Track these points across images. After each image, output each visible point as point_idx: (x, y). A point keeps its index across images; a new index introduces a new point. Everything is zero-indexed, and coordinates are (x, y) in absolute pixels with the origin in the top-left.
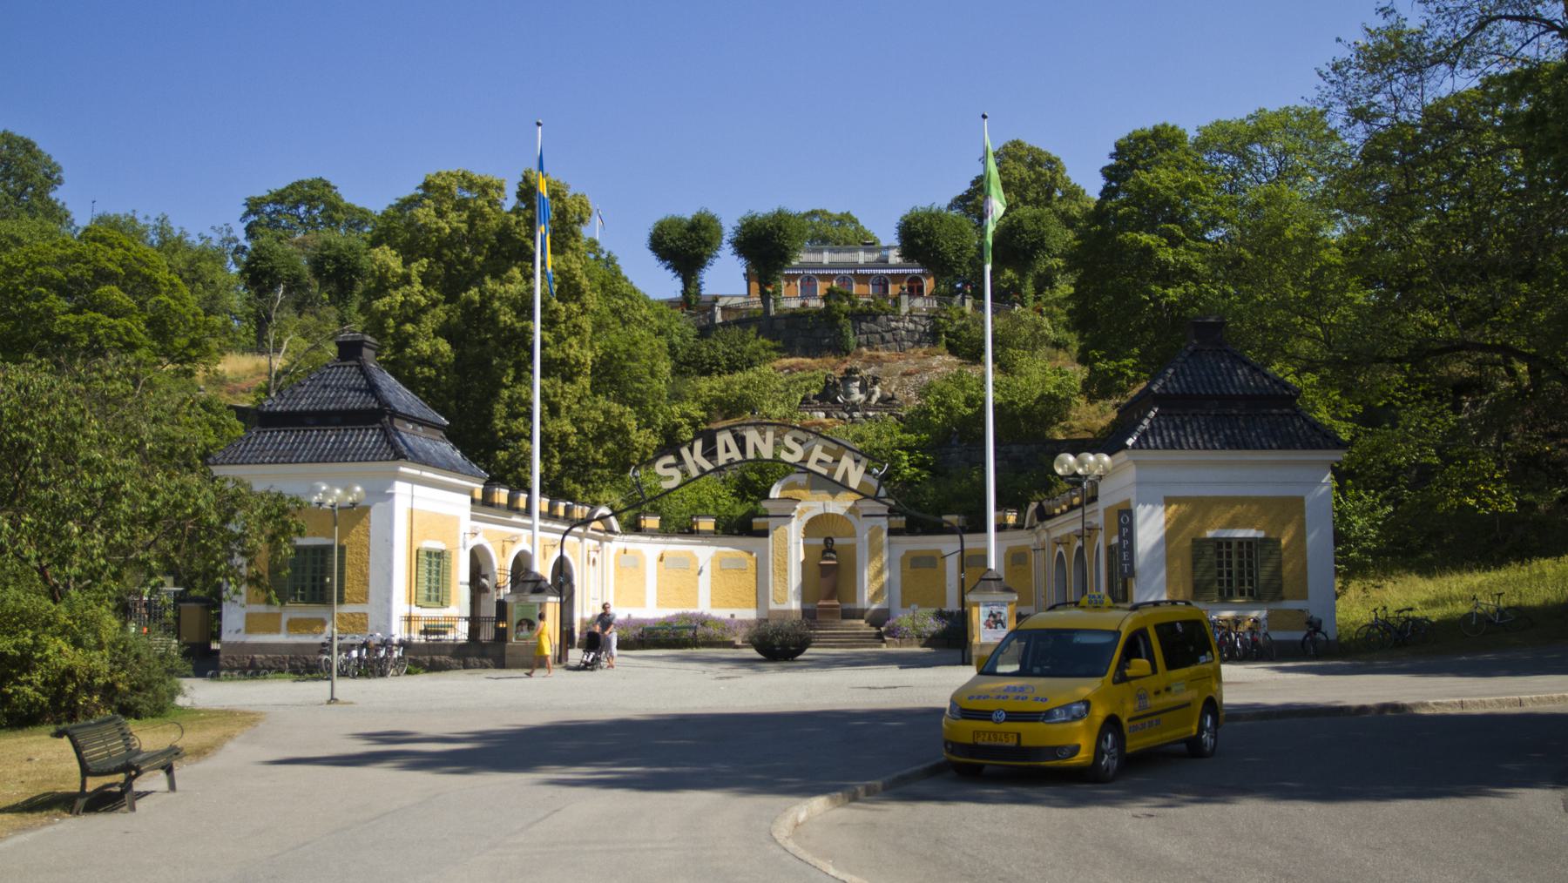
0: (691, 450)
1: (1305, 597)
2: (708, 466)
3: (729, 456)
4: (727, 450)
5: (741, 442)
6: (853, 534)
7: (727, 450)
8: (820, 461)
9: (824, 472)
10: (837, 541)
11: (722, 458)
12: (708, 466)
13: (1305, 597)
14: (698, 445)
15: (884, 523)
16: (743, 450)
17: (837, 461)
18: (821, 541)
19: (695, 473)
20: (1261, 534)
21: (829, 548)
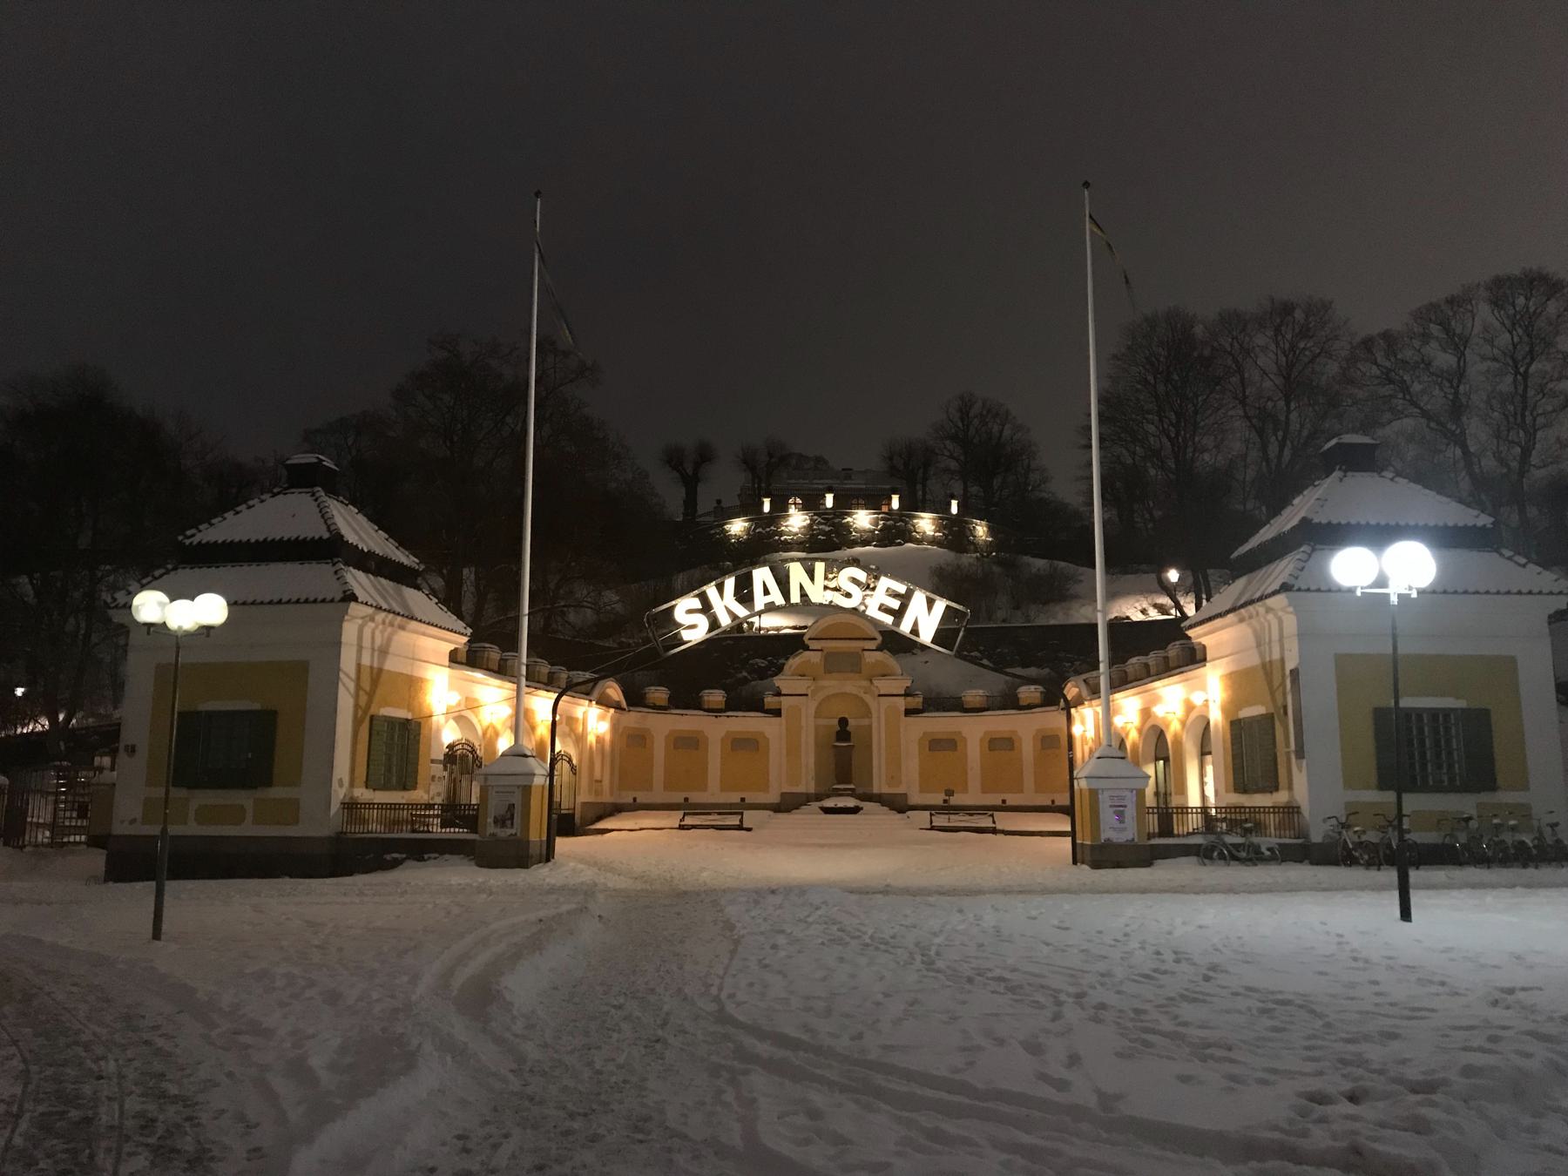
0: (720, 588)
1: (1526, 788)
2: (742, 612)
3: (768, 599)
4: (766, 592)
5: (783, 583)
6: (868, 714)
7: (766, 592)
8: (884, 609)
9: (888, 620)
10: (852, 722)
11: (760, 601)
12: (742, 612)
13: (1526, 788)
14: (730, 583)
15: (901, 703)
16: (786, 593)
17: (904, 607)
18: (836, 722)
19: (725, 621)
20: (1461, 704)
21: (843, 732)
